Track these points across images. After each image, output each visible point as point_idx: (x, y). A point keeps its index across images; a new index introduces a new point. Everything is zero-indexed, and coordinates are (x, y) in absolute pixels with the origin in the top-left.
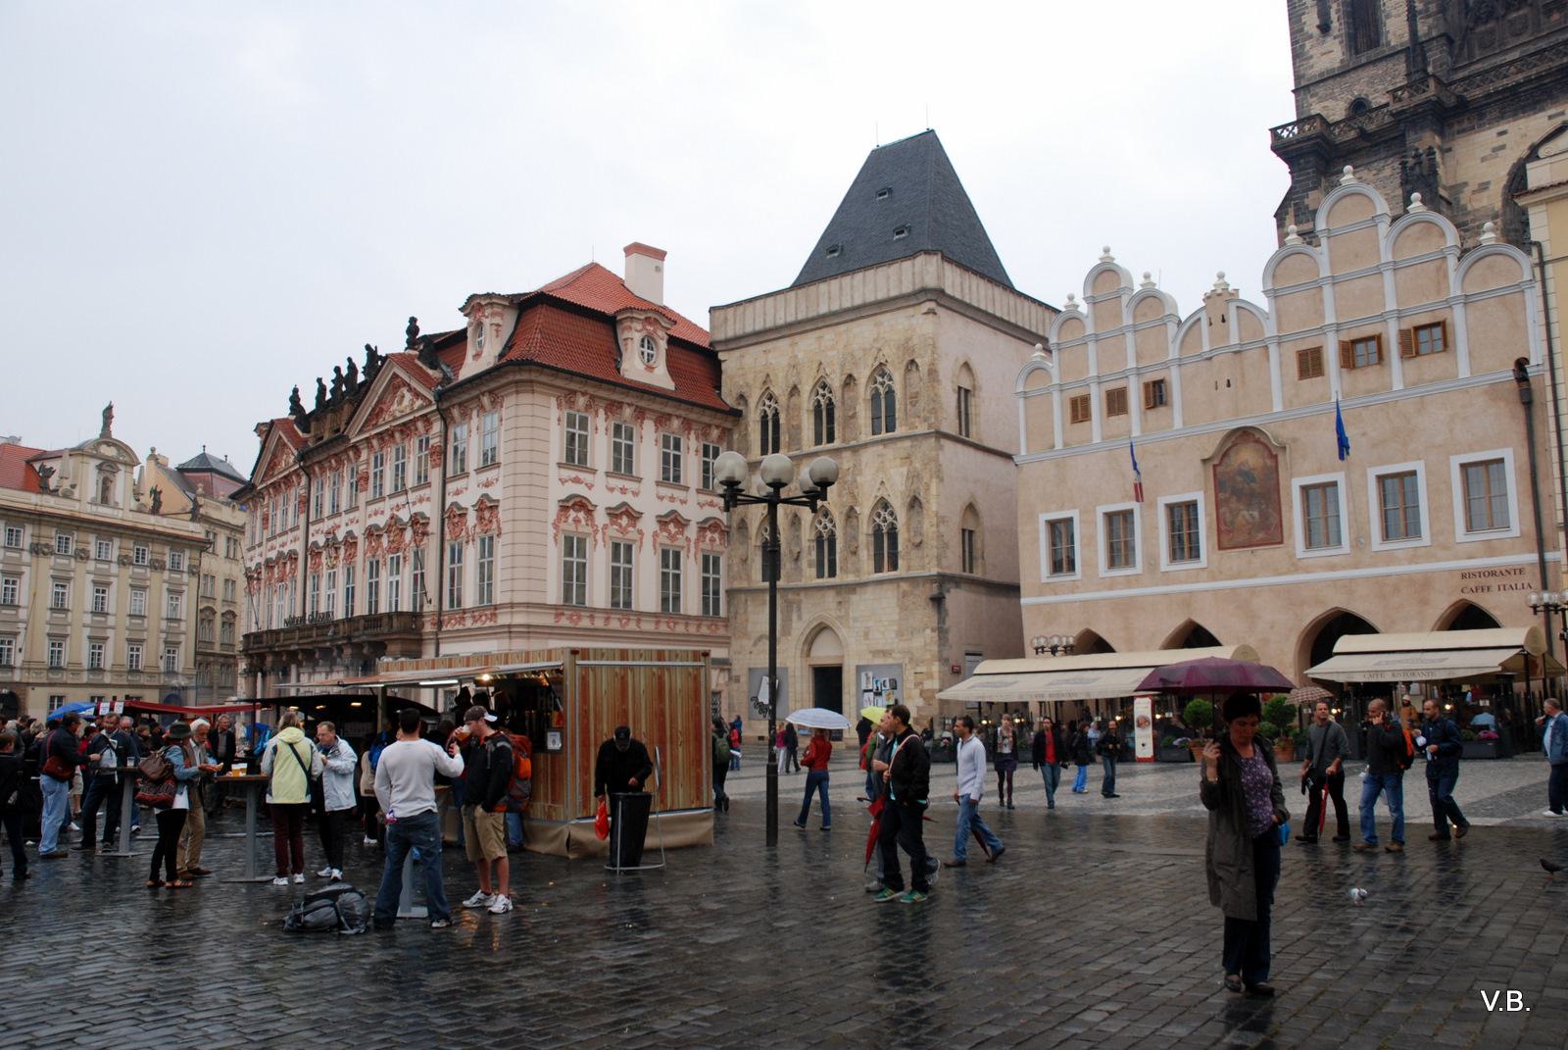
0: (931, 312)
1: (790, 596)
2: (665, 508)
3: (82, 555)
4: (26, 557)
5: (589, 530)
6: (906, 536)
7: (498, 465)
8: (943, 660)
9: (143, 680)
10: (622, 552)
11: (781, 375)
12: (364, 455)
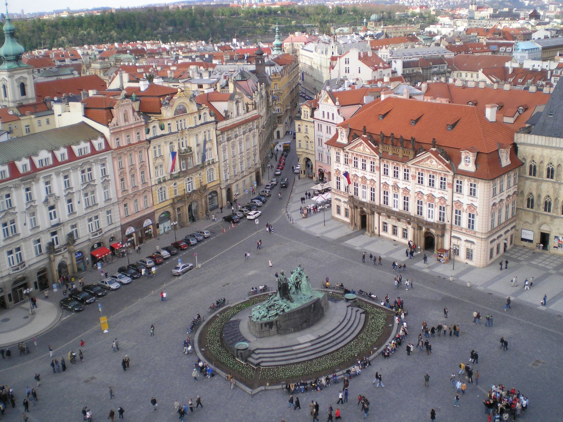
11: (538, 157)
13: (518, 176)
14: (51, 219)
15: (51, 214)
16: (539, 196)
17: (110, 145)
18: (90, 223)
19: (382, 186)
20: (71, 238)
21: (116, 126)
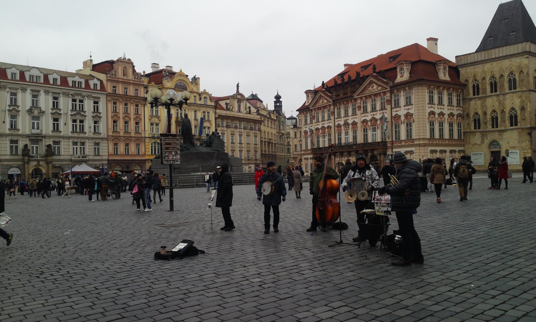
0: (528, 57)
1: (484, 133)
2: (449, 112)
3: (236, 127)
4: (225, 129)
5: (434, 119)
6: (520, 117)
7: (412, 105)
8: (532, 149)
9: (251, 162)
10: (441, 124)
11: (479, 74)
12: (359, 101)
13: (463, 99)
14: (33, 128)
15: (33, 123)
16: (485, 113)
17: (106, 88)
18: (75, 147)
19: (336, 129)
20: (50, 151)
21: (114, 76)
